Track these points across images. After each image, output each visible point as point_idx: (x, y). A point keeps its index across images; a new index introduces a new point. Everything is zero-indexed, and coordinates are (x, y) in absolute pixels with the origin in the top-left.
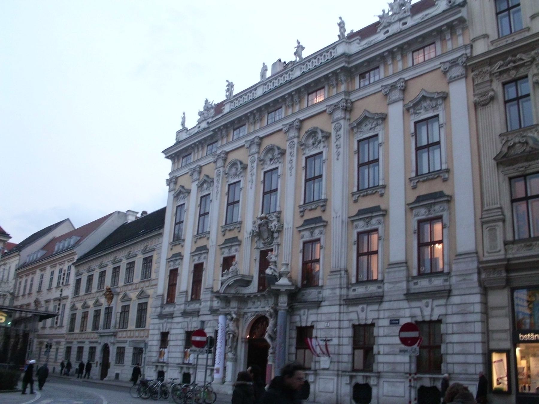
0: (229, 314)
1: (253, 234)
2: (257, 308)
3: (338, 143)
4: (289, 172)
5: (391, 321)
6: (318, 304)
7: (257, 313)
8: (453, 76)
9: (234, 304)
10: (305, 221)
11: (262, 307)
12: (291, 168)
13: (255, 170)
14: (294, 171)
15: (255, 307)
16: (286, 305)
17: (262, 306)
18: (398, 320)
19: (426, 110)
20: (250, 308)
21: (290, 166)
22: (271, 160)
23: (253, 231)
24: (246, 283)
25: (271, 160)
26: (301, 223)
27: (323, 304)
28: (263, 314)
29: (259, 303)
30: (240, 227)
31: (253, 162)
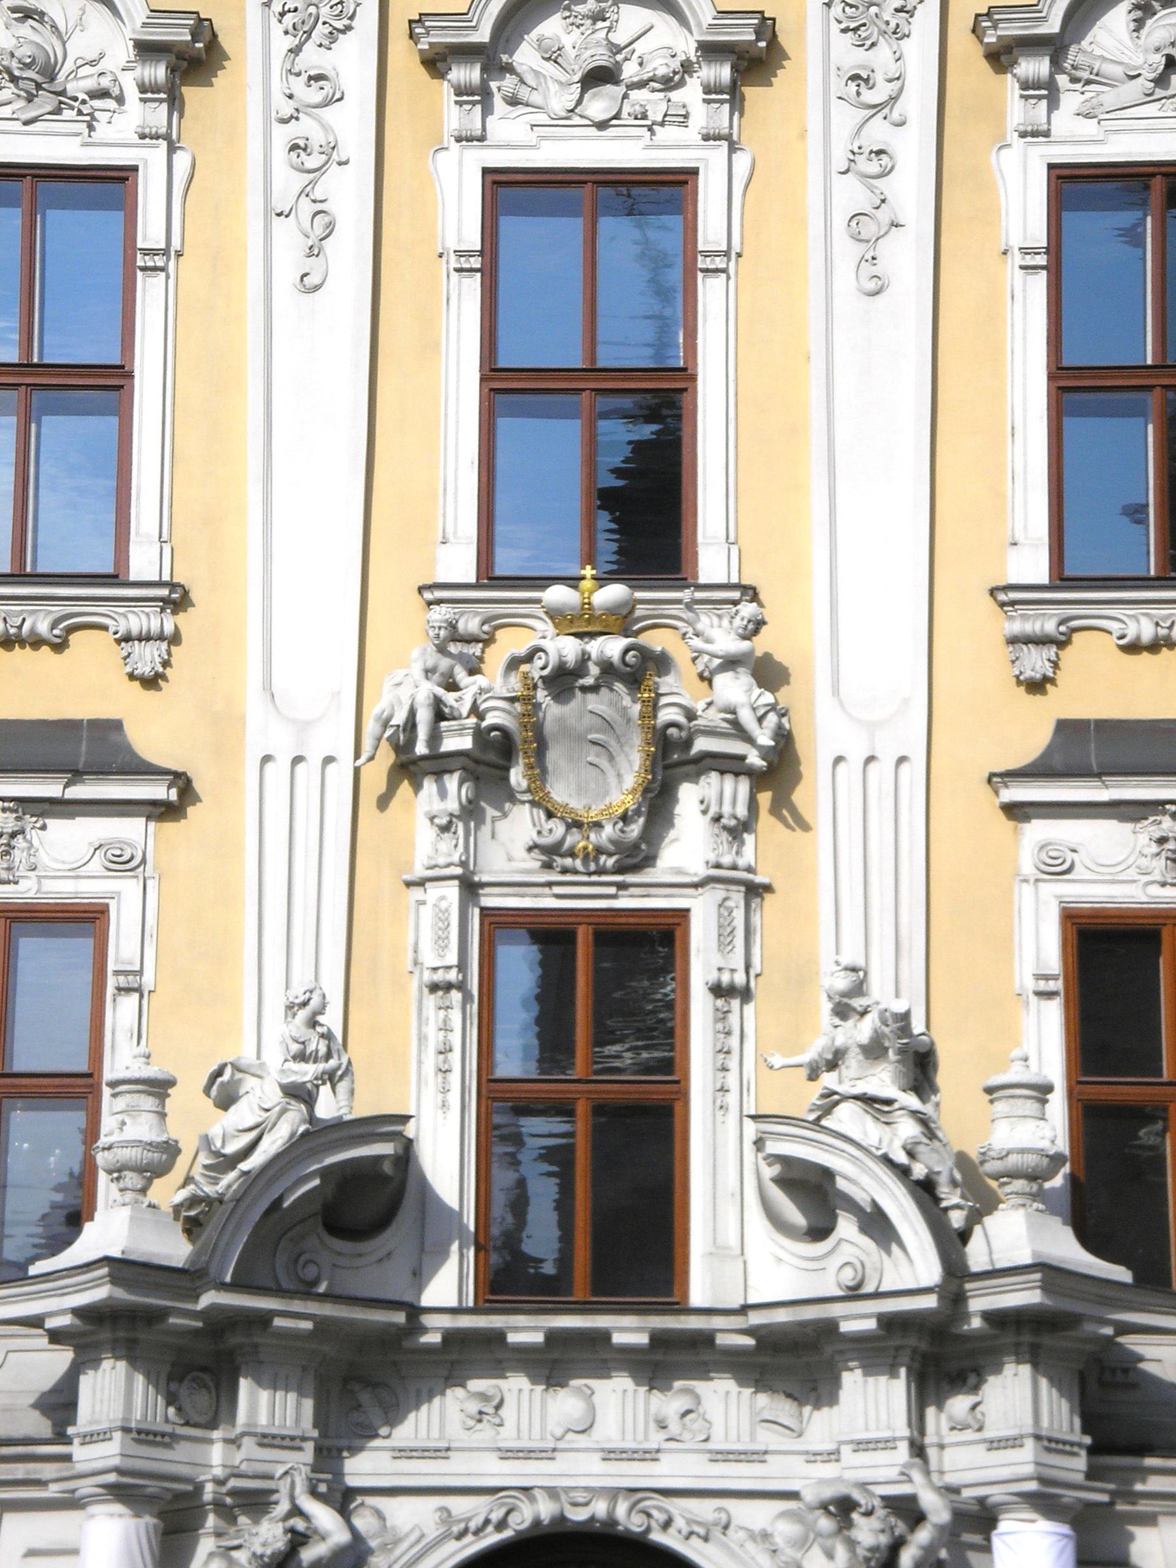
0: (255, 1502)
1: (435, 738)
4: (846, 252)
7: (545, 1509)
10: (1065, 728)
11: (610, 1455)
12: (869, 228)
13: (352, 124)
14: (906, 259)
15: (508, 1437)
16: (1080, 1463)
20: (442, 1452)
21: (850, 195)
22: (599, 77)
23: (440, 714)
24: (354, 1194)
25: (599, 77)
26: (1029, 731)
28: (635, 1524)
30: (175, 639)
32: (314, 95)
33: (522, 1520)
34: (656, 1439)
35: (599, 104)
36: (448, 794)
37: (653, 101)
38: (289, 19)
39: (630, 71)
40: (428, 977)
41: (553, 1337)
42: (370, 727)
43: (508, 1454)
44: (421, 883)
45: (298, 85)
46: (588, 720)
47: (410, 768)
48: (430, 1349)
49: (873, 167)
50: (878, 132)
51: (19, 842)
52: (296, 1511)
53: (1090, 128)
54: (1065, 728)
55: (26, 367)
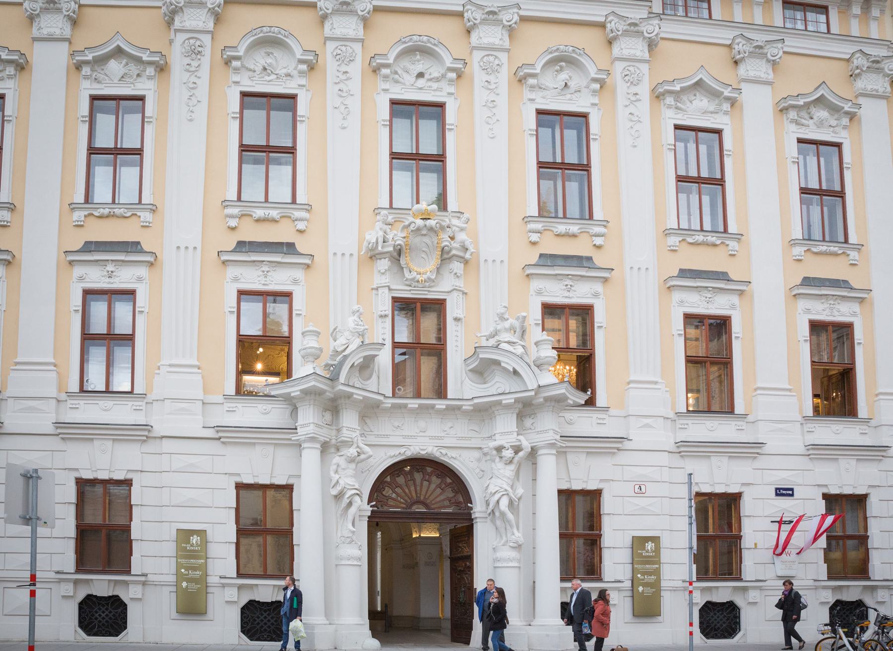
0: (348, 444)
2: (414, 437)
3: (632, 109)
5: (776, 489)
6: (613, 445)
8: (869, 87)
9: (349, 420)
10: (541, 255)
17: (429, 433)
18: (792, 490)
19: (820, 124)
20: (387, 436)
22: (421, 75)
25: (421, 75)
27: (627, 445)
29: (422, 424)
31: (344, 59)
32: (344, 77)
33: (409, 454)
34: (443, 434)
35: (421, 82)
36: (384, 264)
37: (435, 85)
38: (338, 57)
39: (427, 76)
40: (380, 313)
41: (420, 405)
42: (365, 244)
43: (405, 437)
44: (377, 289)
45: (340, 74)
46: (424, 245)
47: (373, 256)
48: (386, 410)
49: (491, 105)
50: (492, 97)
51: (269, 274)
52: (358, 447)
53: (544, 101)
54: (541, 255)
55: (268, 146)
